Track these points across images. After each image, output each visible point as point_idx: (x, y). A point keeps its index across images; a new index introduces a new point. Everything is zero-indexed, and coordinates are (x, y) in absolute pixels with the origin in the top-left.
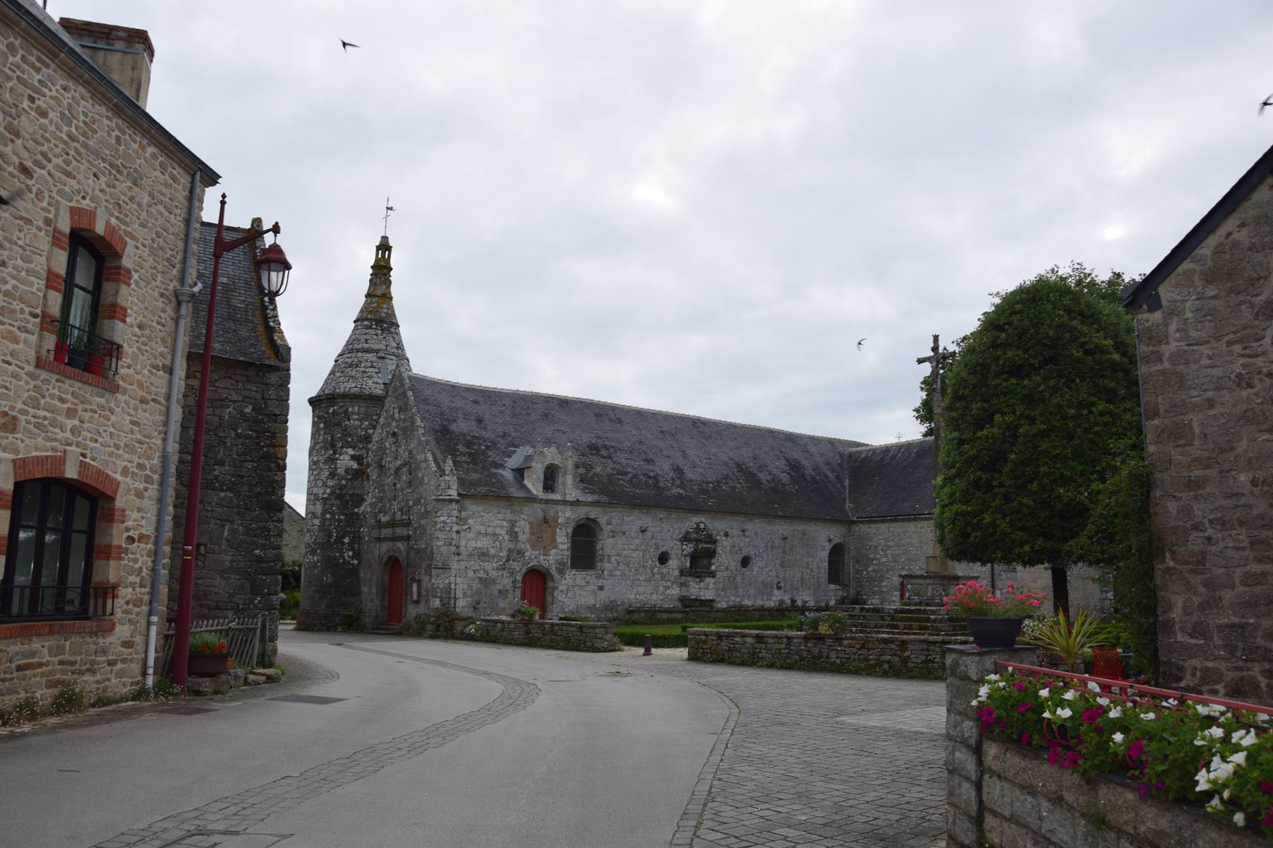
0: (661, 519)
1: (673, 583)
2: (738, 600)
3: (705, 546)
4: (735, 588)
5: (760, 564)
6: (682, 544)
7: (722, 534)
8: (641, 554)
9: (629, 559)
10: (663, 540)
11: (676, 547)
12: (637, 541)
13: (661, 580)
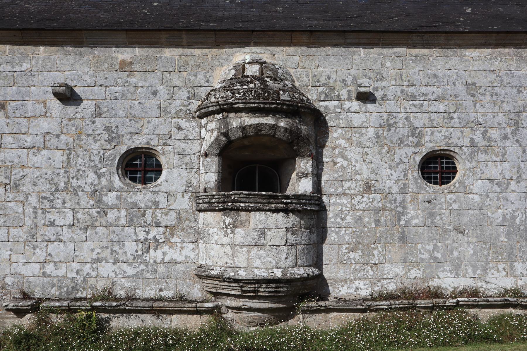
0: (123, 65)
1: (172, 230)
2: (414, 273)
3: (249, 120)
4: (403, 240)
5: (494, 172)
6: (200, 127)
7: (344, 94)
8: (58, 156)
9: (17, 173)
10: (133, 118)
11: (180, 135)
12: (45, 125)
13: (131, 223)
